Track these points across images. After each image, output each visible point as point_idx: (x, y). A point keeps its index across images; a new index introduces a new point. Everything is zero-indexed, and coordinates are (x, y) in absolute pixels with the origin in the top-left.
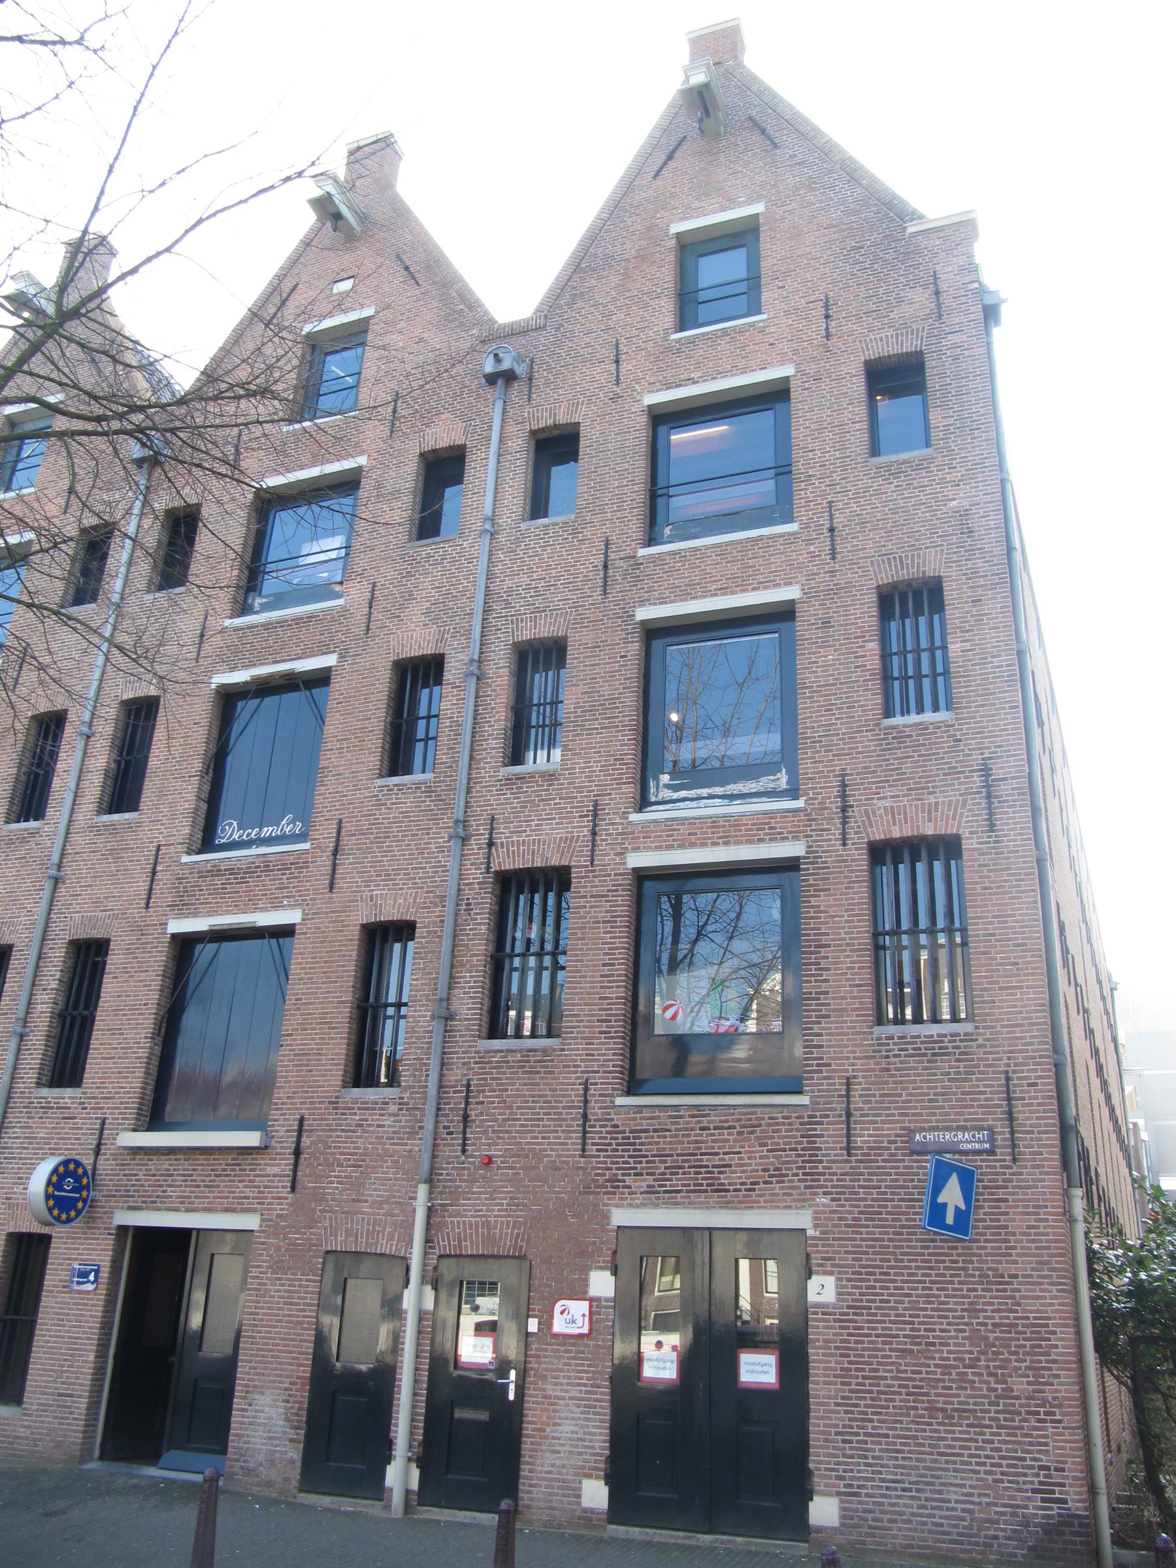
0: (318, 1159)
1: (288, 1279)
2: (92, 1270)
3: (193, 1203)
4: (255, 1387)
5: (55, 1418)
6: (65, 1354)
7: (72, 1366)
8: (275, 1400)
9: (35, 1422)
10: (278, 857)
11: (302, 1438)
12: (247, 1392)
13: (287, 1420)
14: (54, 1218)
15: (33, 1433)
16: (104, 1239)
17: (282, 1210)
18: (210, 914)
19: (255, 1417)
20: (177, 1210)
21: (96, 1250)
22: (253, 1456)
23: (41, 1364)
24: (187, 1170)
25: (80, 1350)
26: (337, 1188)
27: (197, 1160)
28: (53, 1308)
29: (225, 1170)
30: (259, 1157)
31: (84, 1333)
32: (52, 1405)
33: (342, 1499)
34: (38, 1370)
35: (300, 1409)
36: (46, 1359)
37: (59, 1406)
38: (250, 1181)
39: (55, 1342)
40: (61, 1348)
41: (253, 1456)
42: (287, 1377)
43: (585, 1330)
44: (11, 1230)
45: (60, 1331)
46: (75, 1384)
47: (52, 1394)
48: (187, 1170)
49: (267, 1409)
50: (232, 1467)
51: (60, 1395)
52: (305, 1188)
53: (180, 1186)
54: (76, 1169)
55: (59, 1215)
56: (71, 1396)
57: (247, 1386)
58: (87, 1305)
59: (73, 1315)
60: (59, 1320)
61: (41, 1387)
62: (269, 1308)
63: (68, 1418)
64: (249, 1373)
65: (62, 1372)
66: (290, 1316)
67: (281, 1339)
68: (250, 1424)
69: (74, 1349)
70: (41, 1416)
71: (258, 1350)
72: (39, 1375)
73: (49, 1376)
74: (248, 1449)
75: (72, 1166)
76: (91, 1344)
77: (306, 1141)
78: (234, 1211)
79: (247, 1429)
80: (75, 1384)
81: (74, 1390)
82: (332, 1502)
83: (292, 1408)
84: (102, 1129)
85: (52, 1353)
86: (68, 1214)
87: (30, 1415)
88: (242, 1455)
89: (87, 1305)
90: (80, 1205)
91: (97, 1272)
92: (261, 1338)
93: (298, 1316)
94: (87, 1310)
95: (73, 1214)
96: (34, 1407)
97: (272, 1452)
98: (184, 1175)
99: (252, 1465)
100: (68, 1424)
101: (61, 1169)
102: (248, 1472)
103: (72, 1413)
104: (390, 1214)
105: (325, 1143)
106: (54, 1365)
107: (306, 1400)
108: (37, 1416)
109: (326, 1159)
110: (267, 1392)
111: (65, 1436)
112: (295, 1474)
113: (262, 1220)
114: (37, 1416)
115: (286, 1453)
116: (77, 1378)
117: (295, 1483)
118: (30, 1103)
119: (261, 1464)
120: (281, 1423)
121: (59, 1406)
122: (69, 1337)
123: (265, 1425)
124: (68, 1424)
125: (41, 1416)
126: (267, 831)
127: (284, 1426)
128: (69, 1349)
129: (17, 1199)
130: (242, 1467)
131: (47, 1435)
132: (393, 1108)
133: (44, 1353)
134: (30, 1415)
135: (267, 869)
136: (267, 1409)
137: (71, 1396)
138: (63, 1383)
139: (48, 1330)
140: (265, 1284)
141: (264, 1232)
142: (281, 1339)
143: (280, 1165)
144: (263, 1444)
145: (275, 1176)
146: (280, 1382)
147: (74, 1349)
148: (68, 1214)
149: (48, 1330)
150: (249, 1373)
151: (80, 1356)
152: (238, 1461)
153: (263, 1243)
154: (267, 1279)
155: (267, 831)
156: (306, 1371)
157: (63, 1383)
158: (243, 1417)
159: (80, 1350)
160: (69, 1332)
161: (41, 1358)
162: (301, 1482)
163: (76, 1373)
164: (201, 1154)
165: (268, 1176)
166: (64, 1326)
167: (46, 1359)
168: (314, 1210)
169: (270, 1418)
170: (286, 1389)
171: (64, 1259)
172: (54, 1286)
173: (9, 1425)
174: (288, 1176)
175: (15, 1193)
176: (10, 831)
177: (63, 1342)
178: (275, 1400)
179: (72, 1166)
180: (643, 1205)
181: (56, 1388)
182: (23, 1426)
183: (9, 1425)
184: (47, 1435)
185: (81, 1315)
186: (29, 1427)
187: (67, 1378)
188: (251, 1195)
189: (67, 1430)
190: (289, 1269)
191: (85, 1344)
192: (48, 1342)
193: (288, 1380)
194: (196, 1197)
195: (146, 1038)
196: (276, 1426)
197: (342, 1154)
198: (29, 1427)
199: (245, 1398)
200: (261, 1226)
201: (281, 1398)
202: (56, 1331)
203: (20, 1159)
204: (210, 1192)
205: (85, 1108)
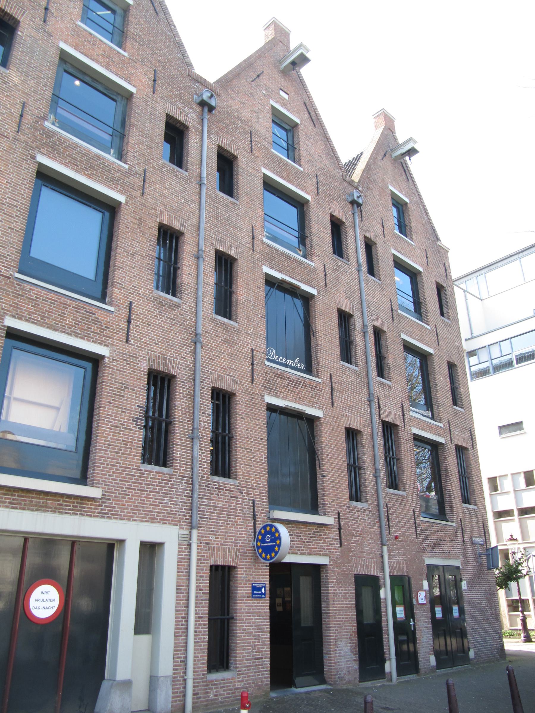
0: (346, 532)
1: (344, 587)
2: (263, 587)
3: (303, 550)
4: (338, 639)
5: (255, 672)
6: (254, 636)
7: (259, 642)
8: (346, 644)
9: (245, 677)
10: (309, 381)
11: (358, 658)
12: (336, 642)
13: (352, 652)
14: (264, 559)
15: (245, 684)
16: (264, 569)
17: (337, 555)
18: (284, 398)
19: (340, 653)
20: (297, 554)
21: (262, 575)
22: (342, 671)
23: (244, 643)
24: (298, 533)
25: (261, 632)
26: (355, 546)
27: (301, 528)
28: (244, 609)
29: (314, 534)
30: (325, 529)
31: (262, 622)
32: (252, 666)
33: (374, 681)
34: (242, 646)
35: (355, 646)
36: (246, 639)
37: (256, 665)
38: (324, 541)
39: (248, 629)
40: (252, 632)
41: (342, 671)
42: (349, 632)
43: (425, 602)
44: (213, 563)
45: (250, 623)
46: (262, 651)
47: (252, 659)
48: (298, 533)
49: (344, 648)
50: (335, 678)
51: (256, 659)
52: (345, 545)
53: (296, 541)
54: (270, 529)
55: (266, 556)
56: (261, 658)
57: (335, 639)
58: (261, 606)
59: (256, 612)
60: (248, 616)
61: (245, 656)
62: (339, 601)
63: (262, 671)
64: (335, 633)
65: (255, 646)
66: (347, 604)
67: (345, 615)
68: (339, 656)
69: (259, 632)
70: (248, 673)
71: (337, 621)
72: (244, 650)
73: (249, 649)
74: (340, 668)
75: (268, 528)
76: (267, 628)
77: (342, 524)
78: (320, 555)
79: (338, 659)
80: (262, 651)
81: (262, 655)
82: (372, 684)
83: (353, 646)
84: (254, 507)
85: (248, 636)
86: (270, 555)
87: (242, 674)
88: (338, 672)
89: (261, 606)
90: (276, 549)
91: (265, 587)
92: (338, 615)
93: (349, 604)
94: (262, 609)
95: (273, 554)
96: (244, 669)
97: (349, 667)
98: (297, 536)
99: (342, 675)
100: (262, 675)
101: (263, 531)
102: (341, 679)
103: (263, 668)
104: (372, 558)
105: (348, 525)
106: (250, 643)
107: (357, 641)
108: (246, 674)
109: (349, 533)
110: (343, 640)
111: (262, 682)
112: (357, 675)
113: (330, 559)
114: (246, 674)
115: (353, 666)
116: (263, 648)
117: (358, 679)
118: (209, 484)
119: (345, 674)
120: (350, 653)
121: (256, 665)
122: (256, 626)
123: (344, 656)
124: (262, 675)
125: (248, 673)
126: (289, 362)
127: (350, 655)
128: (256, 632)
129: (213, 544)
130: (339, 678)
131: (253, 683)
132: (367, 512)
133: (244, 636)
134: (242, 674)
135: (305, 385)
136: (344, 648)
137: (261, 658)
138: (256, 652)
139: (244, 623)
140: (336, 590)
141: (332, 565)
142: (345, 615)
143: (333, 534)
144: (345, 665)
145: (333, 539)
146: (347, 635)
147: (259, 632)
148: (270, 555)
149: (244, 623)
150: (335, 633)
151: (262, 635)
152: (336, 675)
153: (332, 571)
154: (337, 587)
155: (289, 362)
156: (355, 629)
157: (256, 652)
158: (336, 653)
159: (261, 632)
160: (254, 623)
161: (242, 640)
162: (360, 679)
163: (262, 645)
164: (303, 525)
165: (330, 538)
166: (252, 619)
167: (246, 639)
168: (348, 556)
169: (345, 652)
170: (350, 638)
171: (246, 581)
172: (244, 597)
173: (231, 682)
174: (337, 539)
175: (211, 540)
176: (160, 296)
177: (253, 629)
178: (346, 644)
179: (268, 528)
180: (430, 557)
181: (253, 656)
182: (239, 681)
183: (231, 682)
184: (253, 683)
185: (260, 612)
186: (242, 681)
187: (258, 648)
188: (325, 547)
189: (262, 678)
190: (344, 582)
191: (264, 628)
192: (245, 629)
193: (349, 634)
194: (304, 547)
195: (265, 458)
196: (348, 655)
197: (354, 530)
198: (242, 681)
199: (335, 645)
200: (330, 562)
201: (348, 642)
202: (248, 623)
203: (210, 519)
204: (309, 545)
205: (242, 493)
